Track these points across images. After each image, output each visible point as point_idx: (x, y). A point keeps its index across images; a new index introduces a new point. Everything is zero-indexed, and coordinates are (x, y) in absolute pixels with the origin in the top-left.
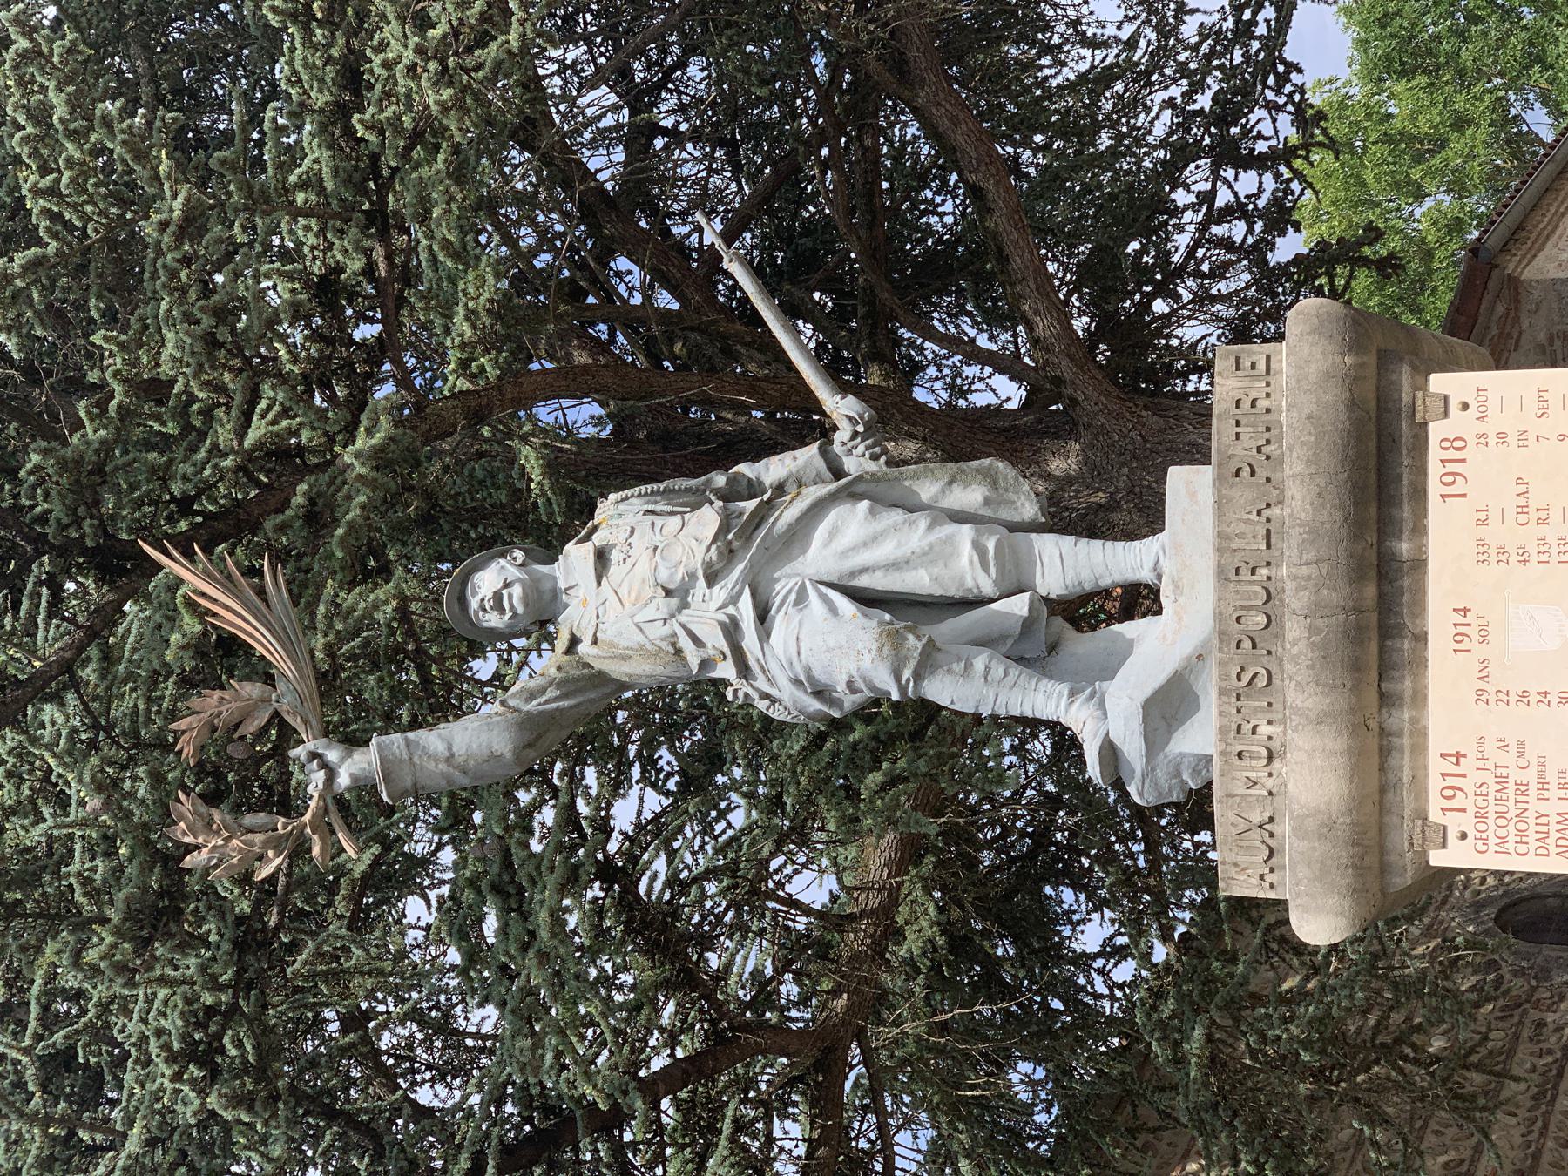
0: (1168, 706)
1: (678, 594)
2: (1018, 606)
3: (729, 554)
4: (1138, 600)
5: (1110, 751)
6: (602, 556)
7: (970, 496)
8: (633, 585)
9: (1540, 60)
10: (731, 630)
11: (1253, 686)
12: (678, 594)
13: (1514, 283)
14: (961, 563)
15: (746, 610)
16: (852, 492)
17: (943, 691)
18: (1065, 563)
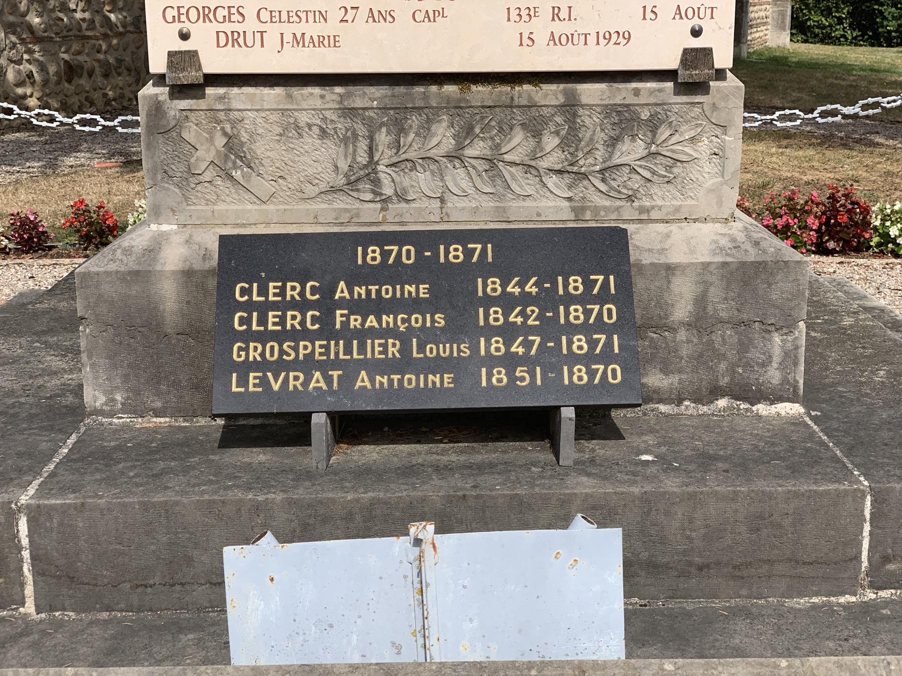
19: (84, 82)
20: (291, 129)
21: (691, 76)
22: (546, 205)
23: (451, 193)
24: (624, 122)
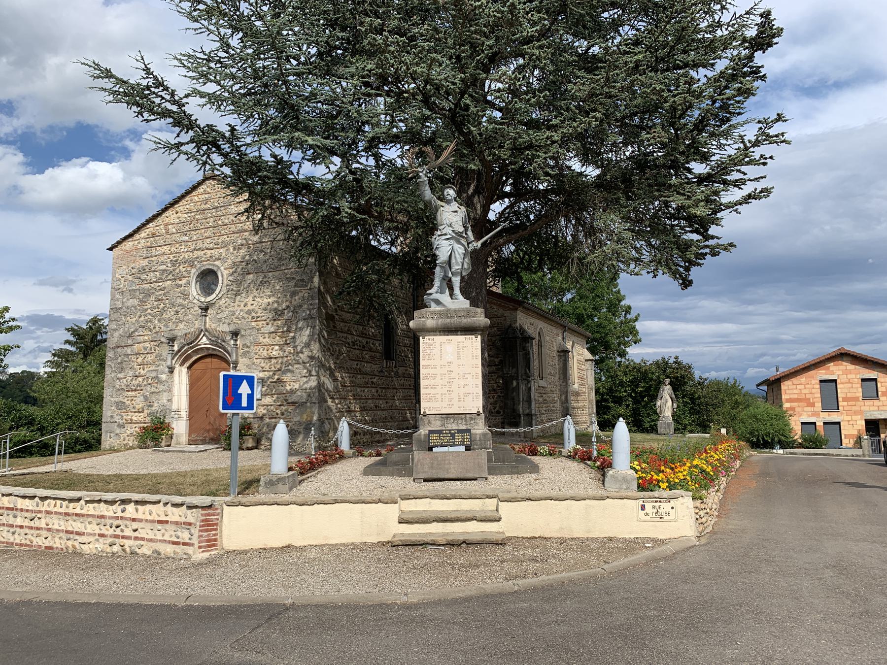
0: (438, 302)
1: (450, 225)
2: (450, 275)
3: (456, 234)
4: (452, 295)
5: (431, 294)
6: (456, 212)
7: (466, 266)
8: (452, 215)
9: (581, 298)
10: (446, 234)
11: (441, 314)
12: (450, 225)
13: (516, 309)
14: (456, 267)
15: (449, 236)
16: (466, 249)
17: (438, 269)
18: (456, 281)
19: (358, 437)
20: (435, 420)
21: (478, 414)
22: (464, 428)
23: (453, 426)
24: (471, 419)
